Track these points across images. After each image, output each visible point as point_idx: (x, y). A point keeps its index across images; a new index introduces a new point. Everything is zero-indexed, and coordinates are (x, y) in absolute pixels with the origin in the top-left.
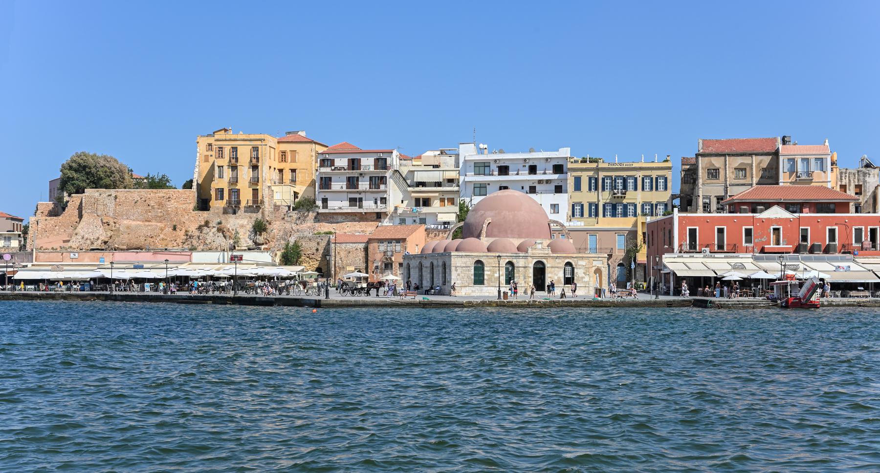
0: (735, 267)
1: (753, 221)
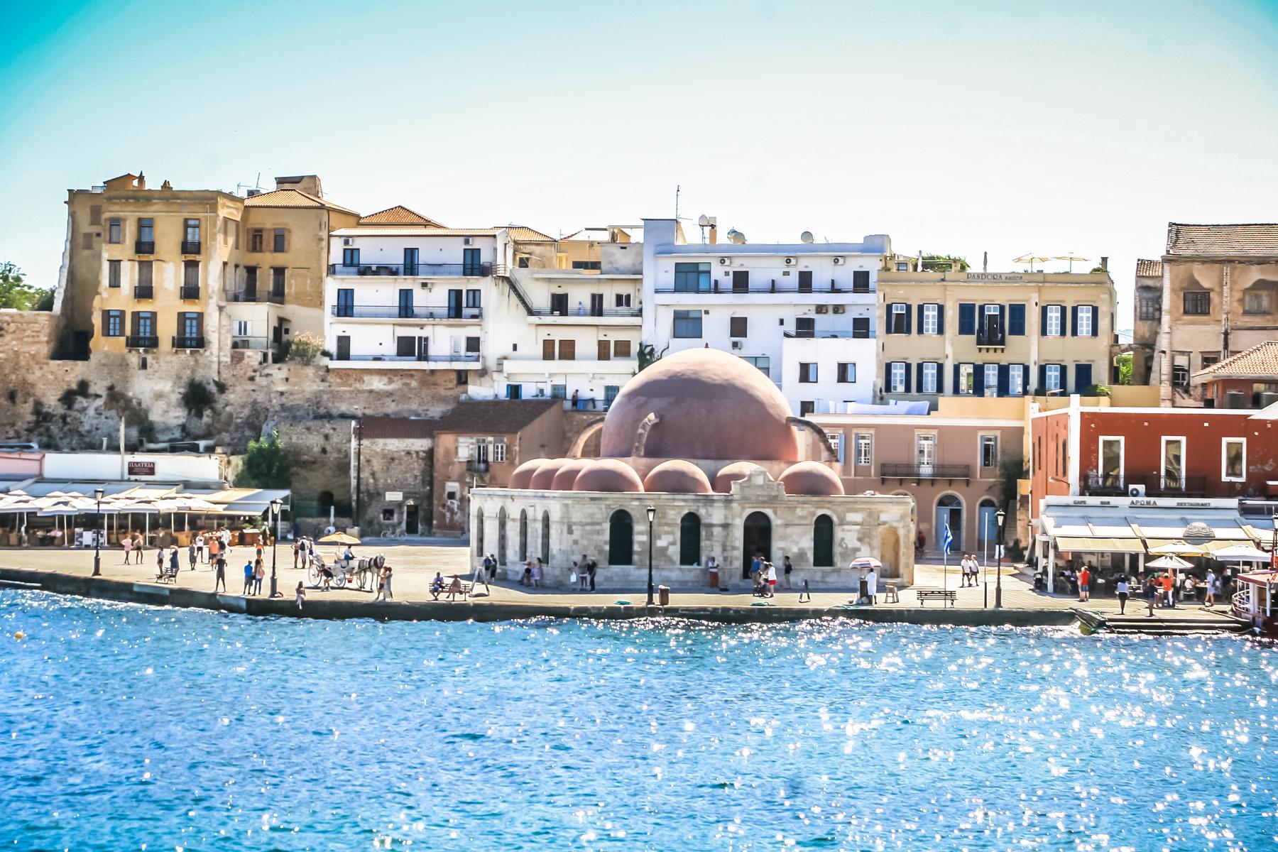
1: (1243, 426)
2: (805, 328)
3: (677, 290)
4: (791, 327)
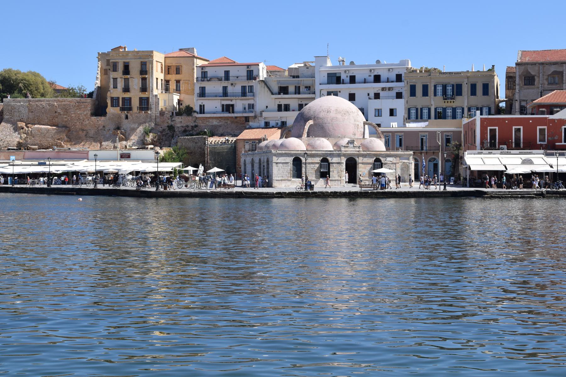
2: (377, 96)
3: (329, 83)
4: (372, 95)
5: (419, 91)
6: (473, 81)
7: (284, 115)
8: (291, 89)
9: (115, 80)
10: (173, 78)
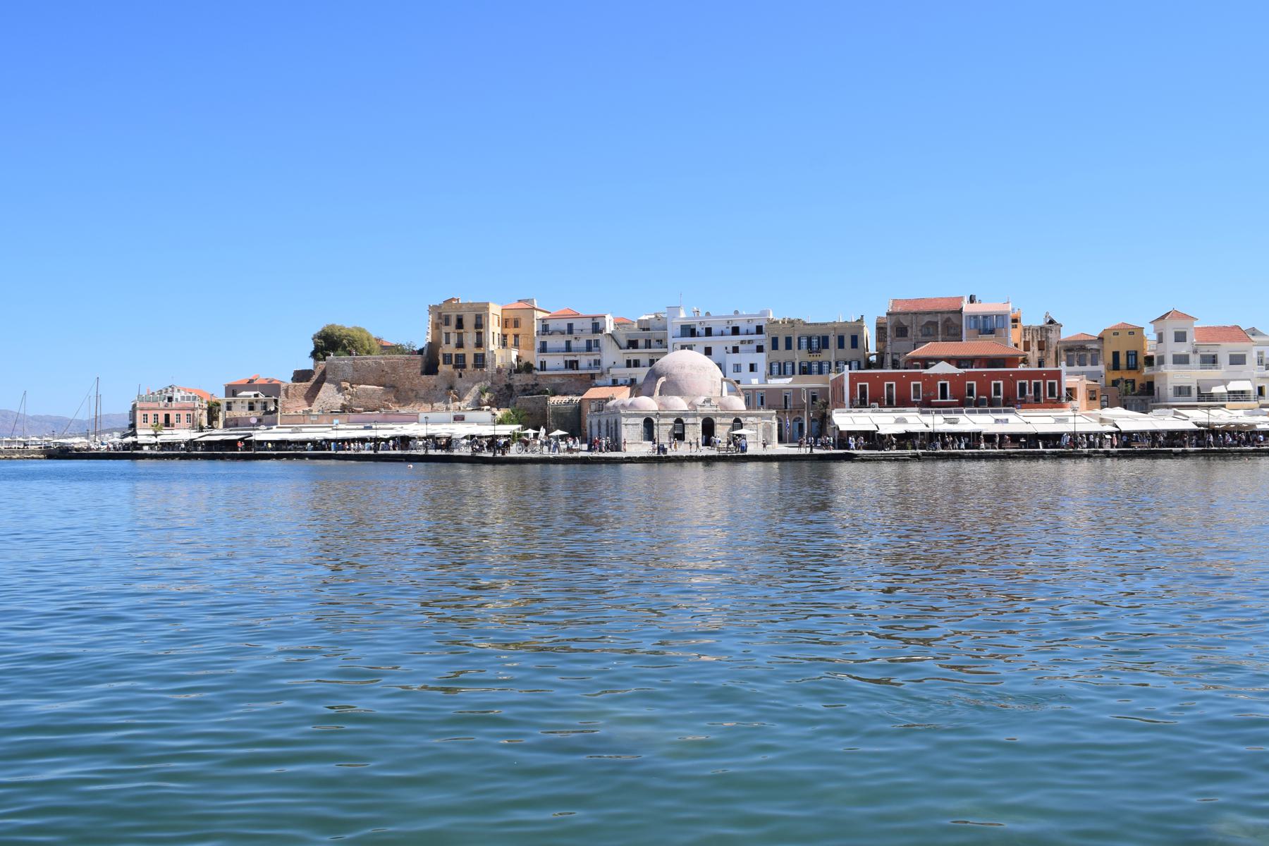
0: (898, 421)
2: (736, 350)
3: (682, 336)
4: (730, 349)
5: (782, 343)
6: (840, 332)
7: (633, 370)
8: (641, 343)
9: (447, 334)
10: (511, 332)
